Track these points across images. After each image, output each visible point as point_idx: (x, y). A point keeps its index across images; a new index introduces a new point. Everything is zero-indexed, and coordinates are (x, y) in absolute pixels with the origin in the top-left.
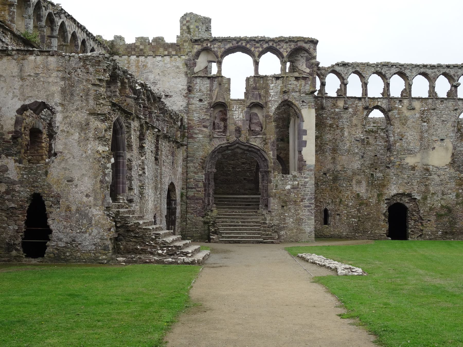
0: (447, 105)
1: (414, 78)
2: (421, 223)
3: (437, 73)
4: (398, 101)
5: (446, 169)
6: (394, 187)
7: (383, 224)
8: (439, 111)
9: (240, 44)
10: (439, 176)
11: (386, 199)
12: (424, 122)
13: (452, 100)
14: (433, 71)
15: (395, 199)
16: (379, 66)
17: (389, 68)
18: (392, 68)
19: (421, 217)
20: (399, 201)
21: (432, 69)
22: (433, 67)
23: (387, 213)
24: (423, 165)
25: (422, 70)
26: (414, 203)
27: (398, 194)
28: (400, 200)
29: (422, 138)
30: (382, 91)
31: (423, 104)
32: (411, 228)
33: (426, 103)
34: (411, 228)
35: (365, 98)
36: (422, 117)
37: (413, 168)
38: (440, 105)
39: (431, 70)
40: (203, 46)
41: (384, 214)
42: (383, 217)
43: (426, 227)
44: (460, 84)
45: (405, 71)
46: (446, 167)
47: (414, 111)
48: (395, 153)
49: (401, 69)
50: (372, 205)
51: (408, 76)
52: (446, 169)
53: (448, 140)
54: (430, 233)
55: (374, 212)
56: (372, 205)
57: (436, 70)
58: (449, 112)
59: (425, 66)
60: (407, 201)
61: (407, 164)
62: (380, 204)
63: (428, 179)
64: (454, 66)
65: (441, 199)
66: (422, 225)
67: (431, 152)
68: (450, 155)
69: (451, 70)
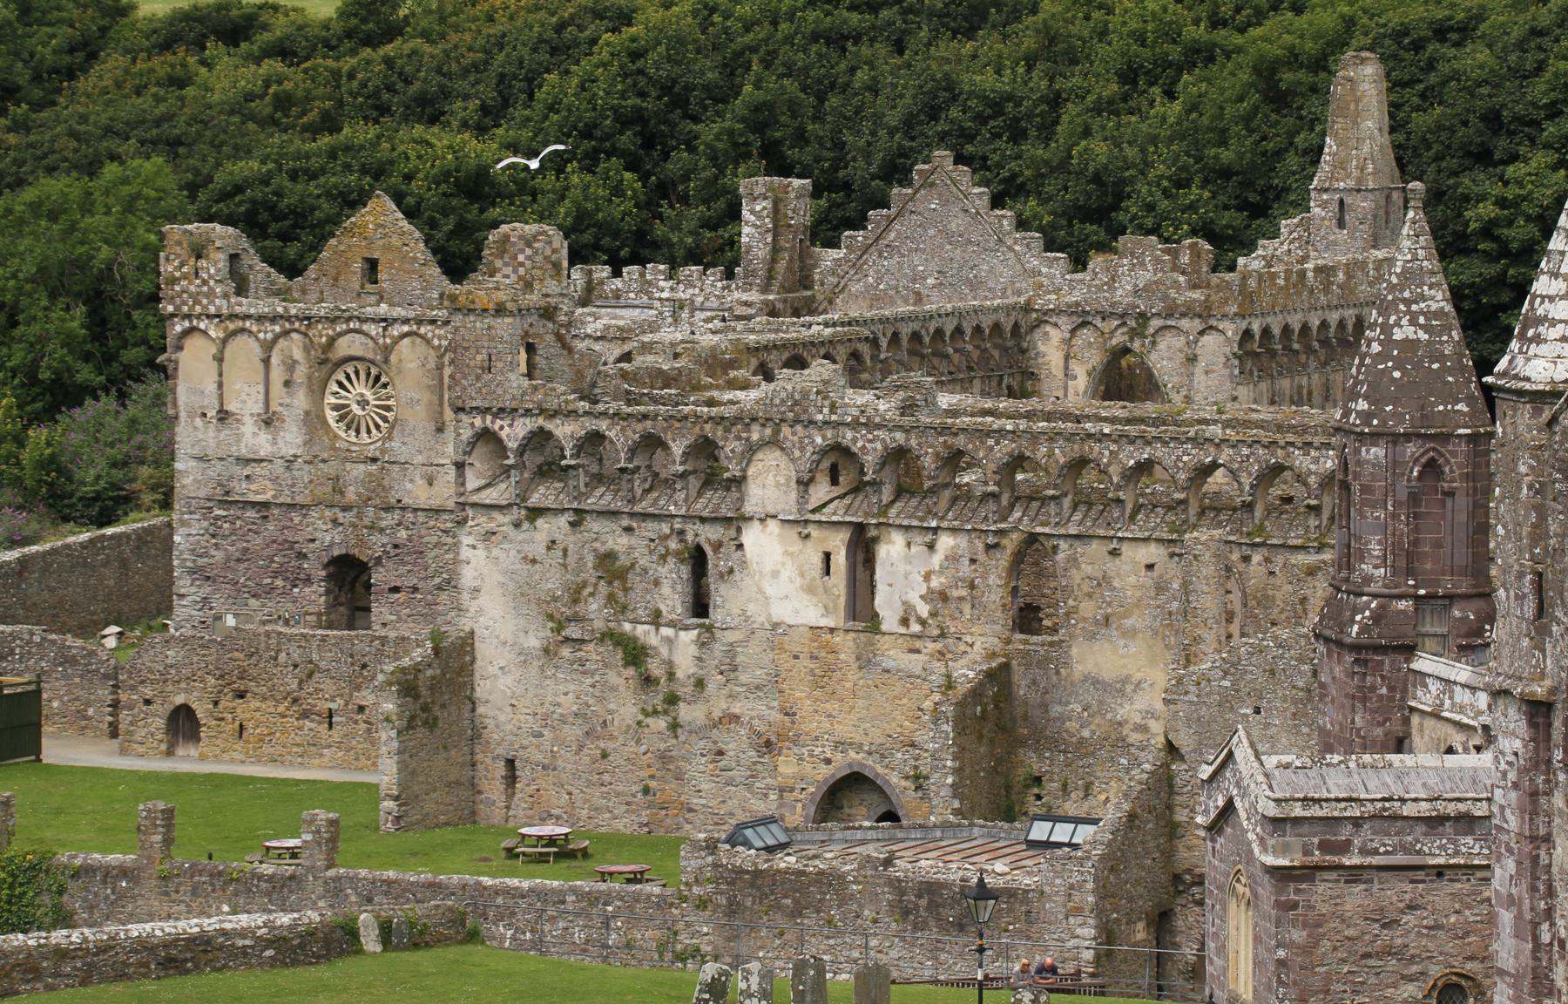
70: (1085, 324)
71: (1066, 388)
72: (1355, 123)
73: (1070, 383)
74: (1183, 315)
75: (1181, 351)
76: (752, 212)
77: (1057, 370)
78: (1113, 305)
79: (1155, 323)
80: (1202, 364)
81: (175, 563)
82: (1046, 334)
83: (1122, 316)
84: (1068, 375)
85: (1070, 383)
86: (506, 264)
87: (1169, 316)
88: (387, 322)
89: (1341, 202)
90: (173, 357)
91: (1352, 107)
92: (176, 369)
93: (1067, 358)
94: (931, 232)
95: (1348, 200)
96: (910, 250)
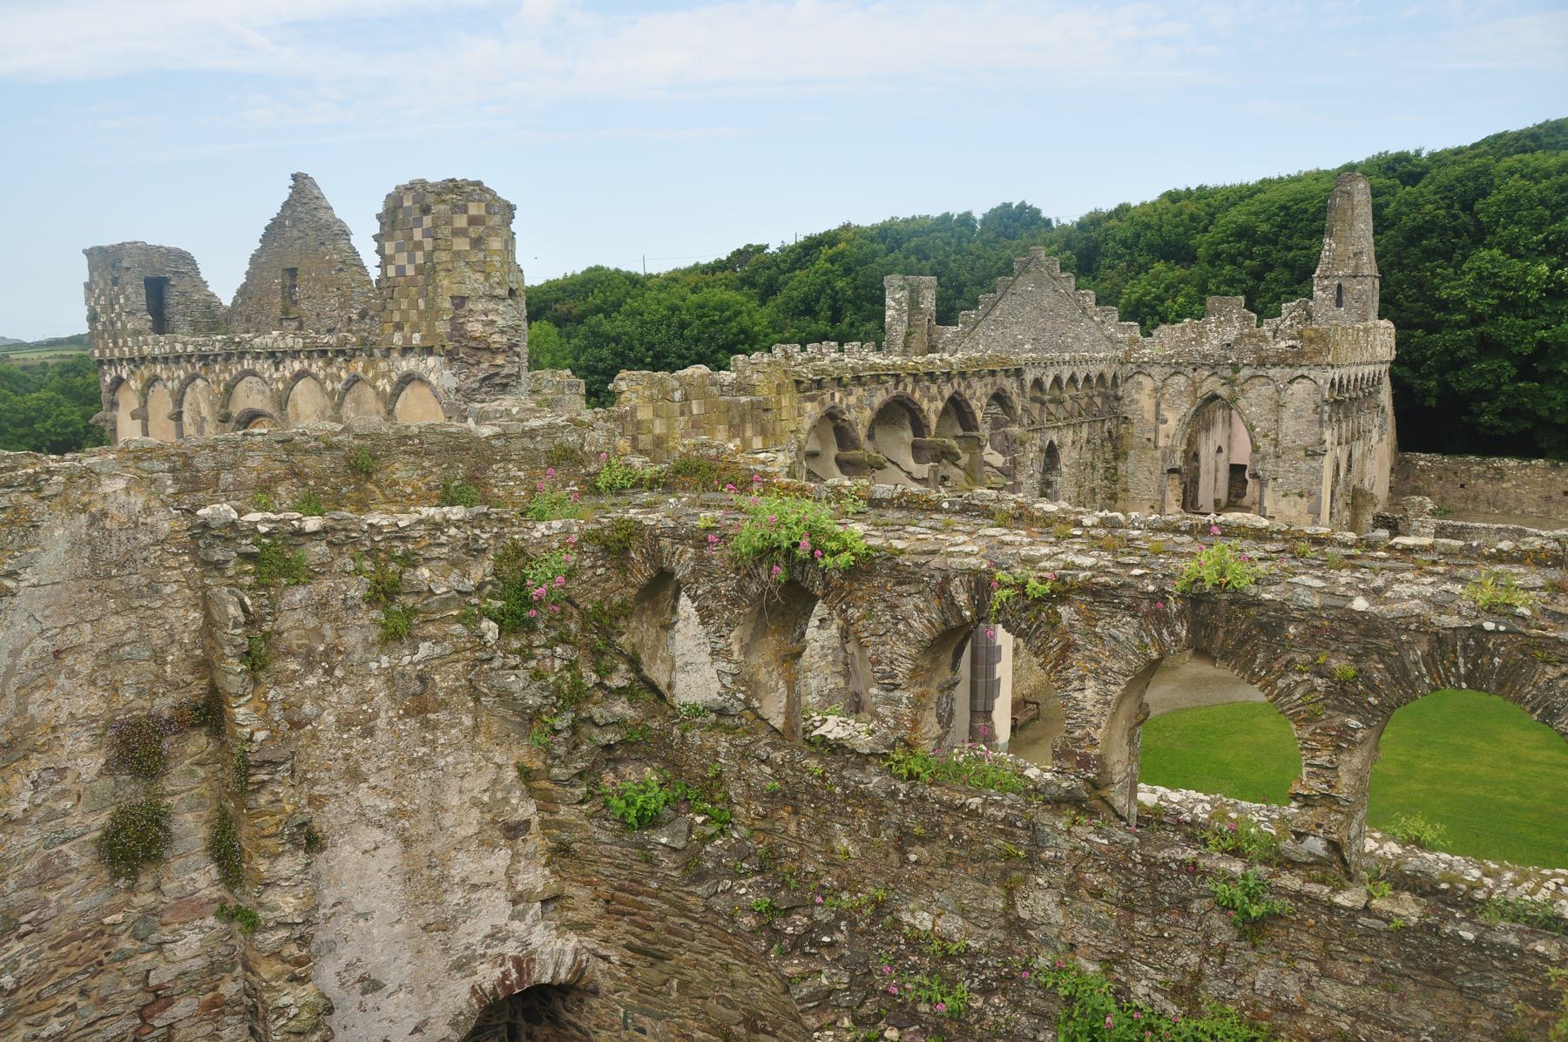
9: (901, 387)
40: (822, 403)
70: (1176, 373)
71: (1156, 431)
72: (1351, 225)
74: (1274, 365)
75: (1271, 399)
76: (894, 300)
77: (1149, 415)
78: (1205, 357)
79: (1245, 372)
82: (1140, 383)
83: (1217, 364)
84: (1160, 419)
85: (1161, 426)
86: (399, 248)
87: (1262, 364)
88: (277, 357)
89: (1340, 286)
90: (109, 415)
91: (1349, 213)
92: (114, 430)
93: (1158, 405)
94: (1028, 309)
95: (1346, 284)
96: (1011, 324)
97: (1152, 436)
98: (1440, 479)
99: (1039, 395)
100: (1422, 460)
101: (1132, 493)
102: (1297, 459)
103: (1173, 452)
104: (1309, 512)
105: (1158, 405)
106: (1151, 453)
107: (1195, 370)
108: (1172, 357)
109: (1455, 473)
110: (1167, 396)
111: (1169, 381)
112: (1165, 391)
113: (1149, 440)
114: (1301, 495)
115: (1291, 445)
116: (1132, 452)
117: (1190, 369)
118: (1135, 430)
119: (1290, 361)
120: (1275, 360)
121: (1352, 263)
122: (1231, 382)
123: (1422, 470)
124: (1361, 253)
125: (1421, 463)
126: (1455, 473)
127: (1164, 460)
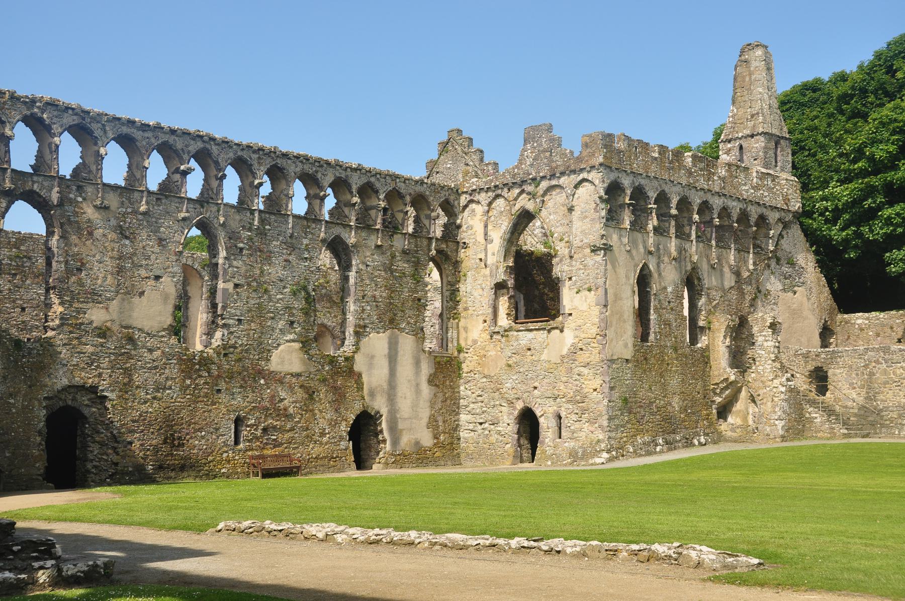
0: (167, 208)
1: (108, 143)
2: (114, 448)
3: (153, 140)
4: (74, 188)
5: (163, 336)
6: (64, 372)
7: (37, 454)
8: (154, 220)
10: (151, 351)
11: (45, 398)
12: (127, 238)
13: (176, 200)
14: (146, 135)
15: (63, 397)
16: (38, 104)
17: (59, 113)
18: (66, 115)
19: (114, 436)
20: (70, 403)
21: (144, 131)
22: (145, 127)
23: (45, 430)
24: (122, 327)
25: (125, 130)
26: (99, 407)
27: (69, 387)
28: (72, 400)
29: (120, 270)
30: (33, 162)
31: (124, 199)
32: (92, 461)
33: (129, 199)
34: (92, 461)
35: (7, 169)
36: (121, 226)
37: (103, 333)
38: (156, 207)
39: (141, 132)
41: (40, 433)
42: (38, 439)
43: (123, 457)
44: (194, 170)
45: (92, 124)
46: (164, 333)
47: (107, 211)
48: (66, 298)
49: (84, 119)
50: (14, 411)
51: (96, 137)
52: (163, 336)
53: (169, 279)
54: (130, 469)
55: (19, 427)
56: (14, 411)
57: (149, 134)
58: (171, 223)
59: (131, 123)
60: (86, 402)
61: (91, 323)
62: (32, 409)
63: (130, 357)
64: (184, 133)
65: (154, 398)
66: (117, 454)
67: (136, 300)
68: (170, 308)
69: (177, 139)
70: (498, 196)
71: (486, 250)
73: (489, 246)
74: (563, 174)
75: (563, 205)
77: (480, 238)
78: (514, 176)
79: (544, 184)
80: (576, 214)
81: (78, 428)
82: (473, 211)
83: (523, 182)
85: (489, 246)
87: (553, 176)
89: (741, 147)
91: (747, 79)
93: (486, 226)
97: (482, 256)
98: (878, 335)
99: (318, 191)
100: (859, 319)
101: (470, 312)
102: (585, 256)
103: (497, 268)
104: (597, 305)
105: (486, 226)
106: (484, 271)
107: (509, 190)
108: (491, 181)
109: (892, 328)
110: (492, 218)
111: (493, 206)
112: (490, 214)
113: (481, 260)
114: (590, 290)
115: (580, 244)
116: (469, 274)
117: (506, 190)
118: (469, 252)
119: (573, 168)
120: (562, 169)
121: (750, 124)
122: (532, 195)
123: (862, 330)
124: (758, 114)
125: (859, 321)
126: (892, 328)
127: (491, 276)
